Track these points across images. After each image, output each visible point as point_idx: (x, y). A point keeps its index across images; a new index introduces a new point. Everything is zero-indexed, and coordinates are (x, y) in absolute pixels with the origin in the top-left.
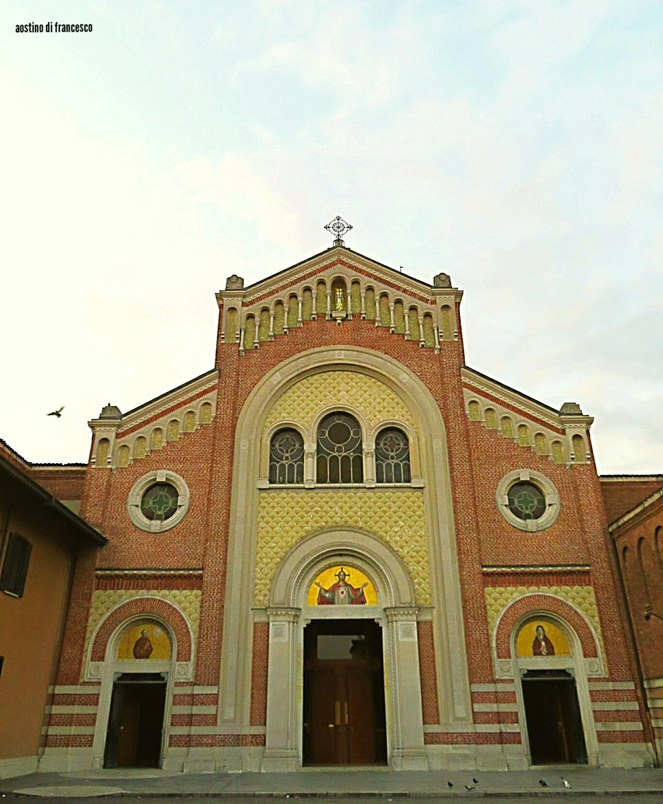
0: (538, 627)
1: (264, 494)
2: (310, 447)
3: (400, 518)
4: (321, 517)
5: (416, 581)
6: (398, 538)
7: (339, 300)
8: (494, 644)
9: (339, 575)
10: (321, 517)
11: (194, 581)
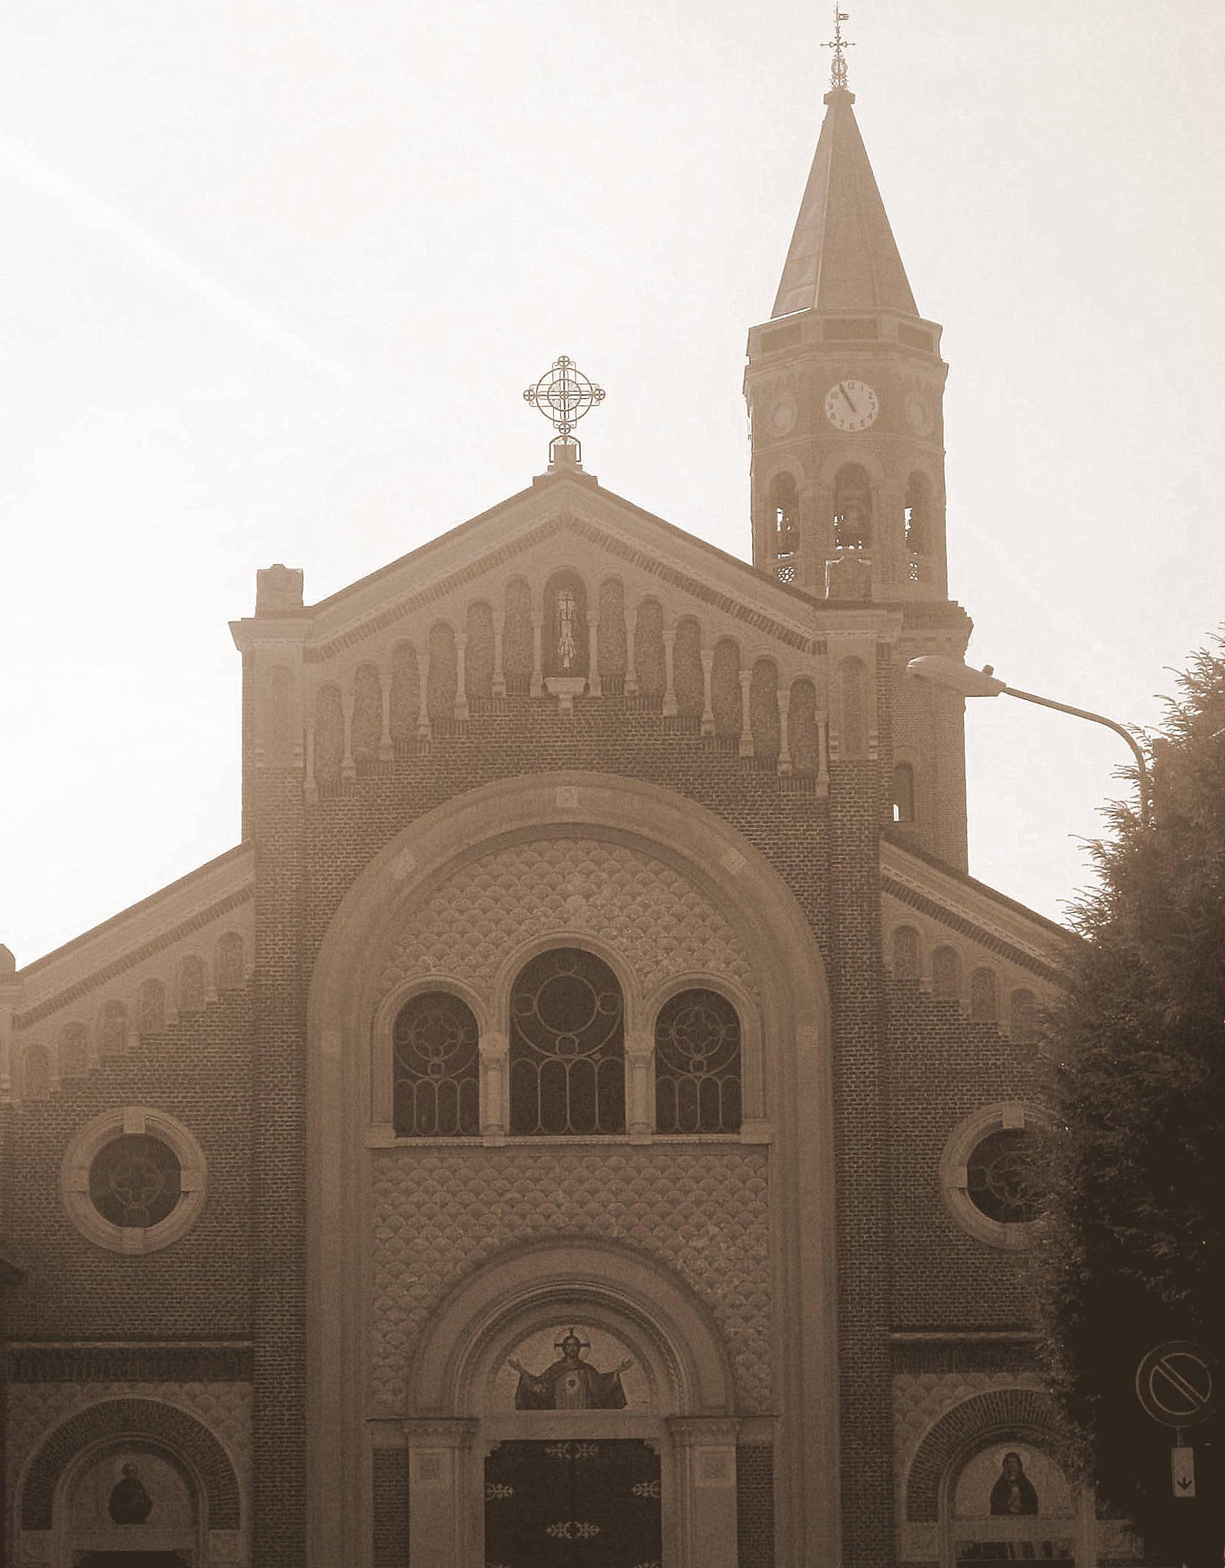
0: (1008, 1456)
1: (384, 1161)
2: (494, 1043)
3: (710, 1216)
4: (523, 1217)
5: (740, 1358)
6: (701, 1263)
7: (566, 630)
8: (903, 1492)
9: (564, 1345)
10: (523, 1217)
11: (233, 1365)
